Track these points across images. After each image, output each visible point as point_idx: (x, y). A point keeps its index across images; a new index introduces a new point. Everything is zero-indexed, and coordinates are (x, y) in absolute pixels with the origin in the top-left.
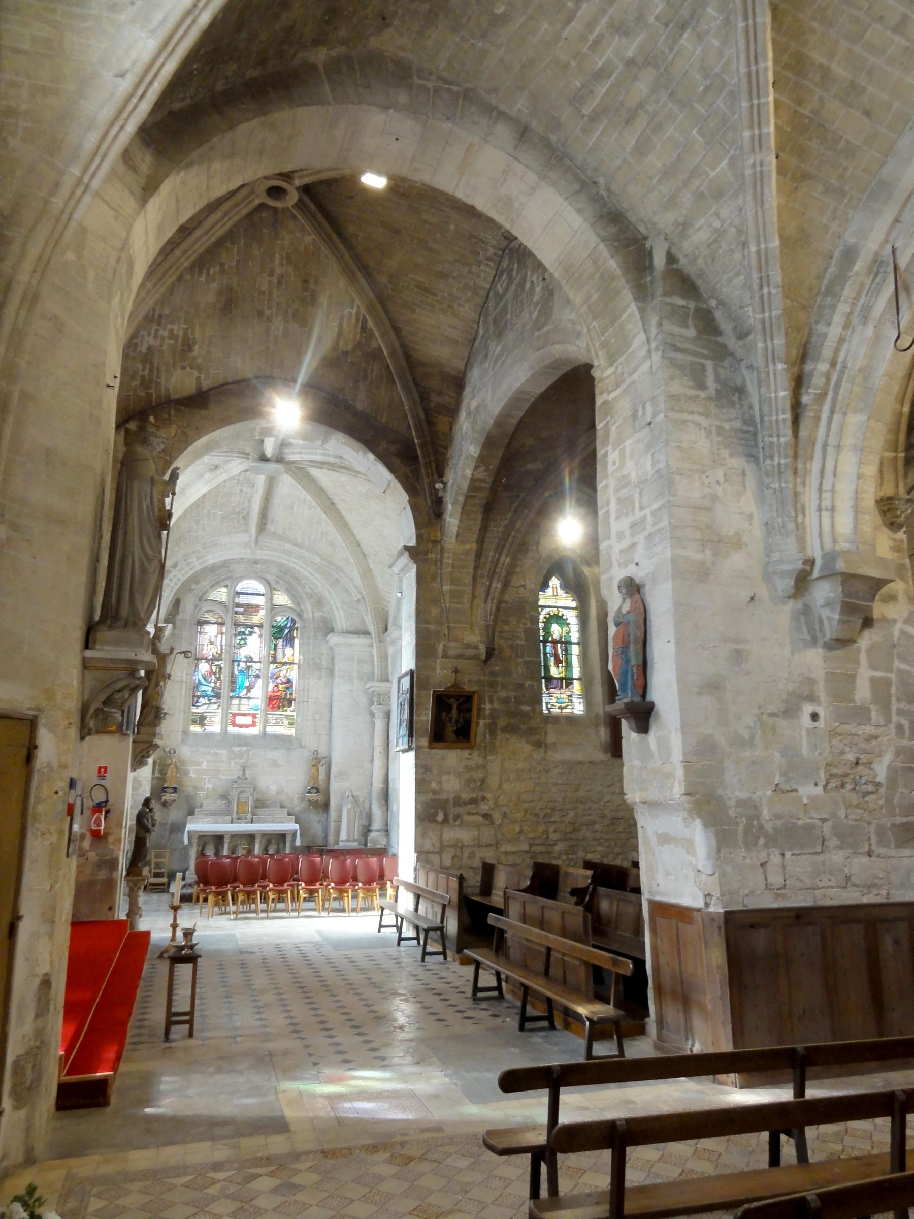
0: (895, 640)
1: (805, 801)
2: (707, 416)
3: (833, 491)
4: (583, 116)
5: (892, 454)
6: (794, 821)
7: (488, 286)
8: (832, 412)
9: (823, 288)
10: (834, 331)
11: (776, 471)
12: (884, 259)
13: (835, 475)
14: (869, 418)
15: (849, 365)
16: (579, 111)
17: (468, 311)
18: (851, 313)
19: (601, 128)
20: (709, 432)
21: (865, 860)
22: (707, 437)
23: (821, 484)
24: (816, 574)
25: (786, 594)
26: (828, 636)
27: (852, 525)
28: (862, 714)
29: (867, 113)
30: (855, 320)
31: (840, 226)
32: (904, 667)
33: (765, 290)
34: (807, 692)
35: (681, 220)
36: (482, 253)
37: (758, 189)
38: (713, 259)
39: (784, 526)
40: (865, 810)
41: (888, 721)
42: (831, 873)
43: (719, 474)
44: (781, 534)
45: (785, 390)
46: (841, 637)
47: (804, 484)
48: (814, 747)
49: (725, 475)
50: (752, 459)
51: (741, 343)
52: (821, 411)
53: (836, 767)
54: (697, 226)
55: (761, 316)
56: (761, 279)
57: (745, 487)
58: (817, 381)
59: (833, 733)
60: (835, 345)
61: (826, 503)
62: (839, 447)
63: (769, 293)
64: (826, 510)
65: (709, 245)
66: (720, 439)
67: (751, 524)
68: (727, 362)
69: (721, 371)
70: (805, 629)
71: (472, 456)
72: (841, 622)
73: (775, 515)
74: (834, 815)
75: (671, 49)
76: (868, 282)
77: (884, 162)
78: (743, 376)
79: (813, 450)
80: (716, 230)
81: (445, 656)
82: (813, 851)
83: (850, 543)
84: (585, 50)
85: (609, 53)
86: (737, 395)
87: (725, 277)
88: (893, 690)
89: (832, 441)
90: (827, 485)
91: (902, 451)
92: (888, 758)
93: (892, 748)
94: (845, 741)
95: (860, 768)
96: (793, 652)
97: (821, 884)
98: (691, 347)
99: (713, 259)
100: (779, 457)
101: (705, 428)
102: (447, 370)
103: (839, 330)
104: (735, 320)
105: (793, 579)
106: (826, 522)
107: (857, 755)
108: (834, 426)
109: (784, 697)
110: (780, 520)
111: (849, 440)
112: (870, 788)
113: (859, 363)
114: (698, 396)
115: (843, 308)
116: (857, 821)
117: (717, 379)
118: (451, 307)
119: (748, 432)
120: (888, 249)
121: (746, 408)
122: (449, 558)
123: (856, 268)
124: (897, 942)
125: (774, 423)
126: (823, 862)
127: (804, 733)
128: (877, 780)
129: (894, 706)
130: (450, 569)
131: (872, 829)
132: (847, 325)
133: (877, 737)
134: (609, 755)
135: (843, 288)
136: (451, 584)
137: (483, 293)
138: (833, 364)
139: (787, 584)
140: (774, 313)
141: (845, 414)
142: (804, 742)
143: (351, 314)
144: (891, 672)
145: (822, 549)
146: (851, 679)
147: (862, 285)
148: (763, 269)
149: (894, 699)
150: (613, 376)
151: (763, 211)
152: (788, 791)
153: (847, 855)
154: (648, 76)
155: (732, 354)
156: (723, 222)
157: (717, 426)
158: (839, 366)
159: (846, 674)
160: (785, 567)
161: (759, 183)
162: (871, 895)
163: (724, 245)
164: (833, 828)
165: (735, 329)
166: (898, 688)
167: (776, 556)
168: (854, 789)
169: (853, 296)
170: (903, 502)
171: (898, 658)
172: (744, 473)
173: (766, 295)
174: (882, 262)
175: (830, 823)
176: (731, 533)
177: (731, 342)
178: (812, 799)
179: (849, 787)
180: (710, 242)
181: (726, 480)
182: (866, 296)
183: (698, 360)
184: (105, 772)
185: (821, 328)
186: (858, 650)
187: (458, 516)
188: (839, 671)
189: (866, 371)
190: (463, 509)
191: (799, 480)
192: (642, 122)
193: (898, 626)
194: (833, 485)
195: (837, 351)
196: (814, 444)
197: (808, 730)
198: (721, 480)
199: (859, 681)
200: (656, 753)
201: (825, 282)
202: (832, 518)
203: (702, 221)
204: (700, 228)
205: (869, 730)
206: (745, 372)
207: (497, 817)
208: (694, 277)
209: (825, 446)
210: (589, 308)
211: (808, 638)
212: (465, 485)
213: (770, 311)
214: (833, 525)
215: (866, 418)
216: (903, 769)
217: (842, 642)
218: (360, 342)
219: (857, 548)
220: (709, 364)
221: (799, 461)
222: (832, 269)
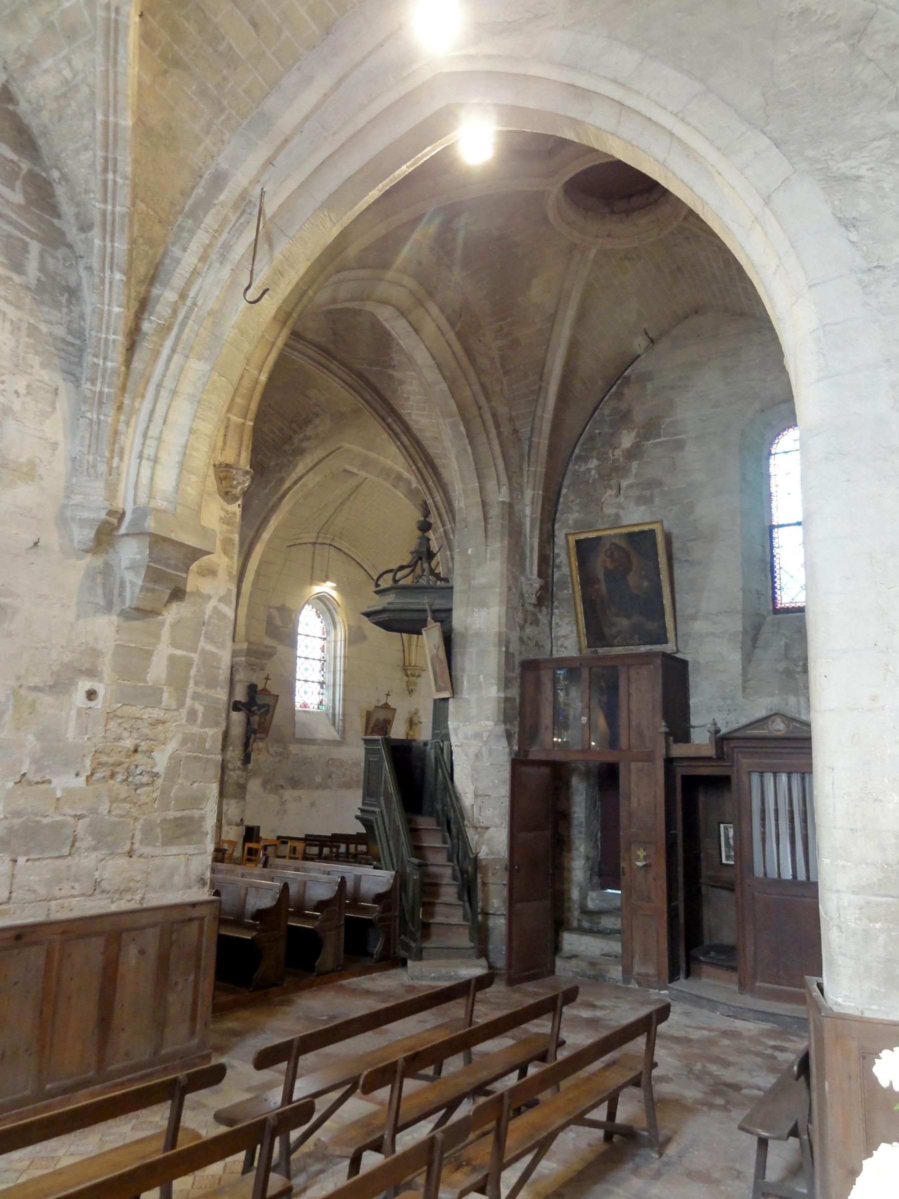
0: (206, 617)
1: (59, 794)
2: (18, 308)
3: (159, 439)
5: (241, 420)
6: (38, 818)
8: (173, 351)
9: (187, 208)
10: (189, 259)
11: (96, 399)
12: (252, 198)
13: (164, 423)
14: (212, 370)
15: (199, 303)
18: (210, 246)
20: (15, 329)
21: (123, 861)
22: (12, 333)
23: (148, 427)
24: (123, 530)
25: (83, 547)
26: (128, 603)
27: (174, 483)
28: (152, 696)
29: (255, 25)
30: (214, 255)
31: (214, 144)
32: (210, 648)
33: (110, 176)
34: (87, 666)
37: (112, 43)
38: (60, 118)
39: (94, 466)
40: (135, 803)
41: (181, 704)
42: (76, 880)
43: (21, 384)
44: (89, 475)
45: (120, 306)
46: (141, 607)
47: (128, 424)
48: (83, 730)
49: (28, 386)
50: (71, 378)
51: (83, 236)
52: (161, 346)
53: (108, 755)
55: (102, 206)
56: (106, 159)
57: (53, 405)
58: (161, 310)
59: (111, 715)
60: (187, 275)
61: (149, 451)
62: (174, 392)
63: (115, 182)
64: (148, 459)
65: (57, 98)
66: (32, 341)
67: (53, 455)
68: (61, 252)
69: (50, 261)
70: (100, 591)
72: (143, 588)
73: (85, 450)
74: (94, 810)
76: (234, 219)
77: (268, 94)
78: (80, 277)
79: (145, 388)
80: (66, 82)
82: (57, 854)
83: (170, 502)
86: (66, 295)
87: (71, 146)
88: (193, 672)
89: (168, 383)
90: (154, 432)
91: (251, 420)
92: (172, 746)
93: (180, 735)
94: (125, 725)
95: (138, 756)
96: (78, 617)
97: (57, 893)
98: (14, 216)
99: (60, 118)
100: (102, 383)
101: (12, 322)
103: (195, 260)
104: (78, 205)
105: (95, 531)
106: (146, 472)
107: (138, 741)
108: (172, 366)
109: (55, 668)
110: (91, 458)
111: (187, 388)
112: (145, 779)
113: (211, 305)
114: (11, 279)
115: (201, 238)
116: (122, 816)
117: (42, 268)
119: (73, 345)
120: (258, 191)
121: (75, 315)
123: (222, 197)
124: (142, 952)
125: (102, 342)
126: (69, 867)
127: (73, 713)
128: (155, 770)
129: (191, 689)
131: (139, 825)
132: (203, 258)
133: (164, 723)
135: (205, 214)
138: (183, 296)
139: (84, 535)
140: (118, 209)
141: (187, 357)
142: (72, 724)
144: (195, 652)
145: (135, 502)
146: (147, 654)
147: (226, 218)
148: (111, 147)
149: (192, 681)
151: (116, 73)
152: (38, 783)
153: (101, 857)
155: (70, 246)
156: (75, 74)
157: (29, 324)
158: (189, 302)
159: (141, 649)
160: (86, 514)
161: (112, 34)
162: (123, 902)
163: (73, 104)
164: (90, 825)
165: (77, 215)
166: (198, 671)
167: (77, 499)
168: (126, 780)
169: (216, 227)
170: (240, 473)
171: (206, 638)
172: (56, 392)
173: (110, 183)
174: (250, 201)
175: (86, 821)
176: (23, 459)
177: (72, 234)
178: (68, 791)
179: (120, 777)
180: (59, 93)
181: (28, 393)
182: (229, 233)
183: (18, 234)
185: (176, 250)
186: (162, 624)
188: (133, 645)
189: (217, 316)
191: (122, 418)
193: (213, 603)
194: (161, 433)
195: (189, 283)
196: (148, 382)
197: (79, 710)
198: (23, 391)
199: (155, 658)
201: (190, 202)
202: (153, 469)
203: (48, 63)
204: (46, 71)
205: (157, 713)
206: (83, 274)
208: (35, 130)
209: (159, 386)
211: (101, 601)
213: (114, 205)
214: (152, 478)
215: (208, 368)
216: (187, 757)
217: (142, 613)
219: (175, 509)
220: (35, 247)
221: (126, 395)
222: (199, 191)
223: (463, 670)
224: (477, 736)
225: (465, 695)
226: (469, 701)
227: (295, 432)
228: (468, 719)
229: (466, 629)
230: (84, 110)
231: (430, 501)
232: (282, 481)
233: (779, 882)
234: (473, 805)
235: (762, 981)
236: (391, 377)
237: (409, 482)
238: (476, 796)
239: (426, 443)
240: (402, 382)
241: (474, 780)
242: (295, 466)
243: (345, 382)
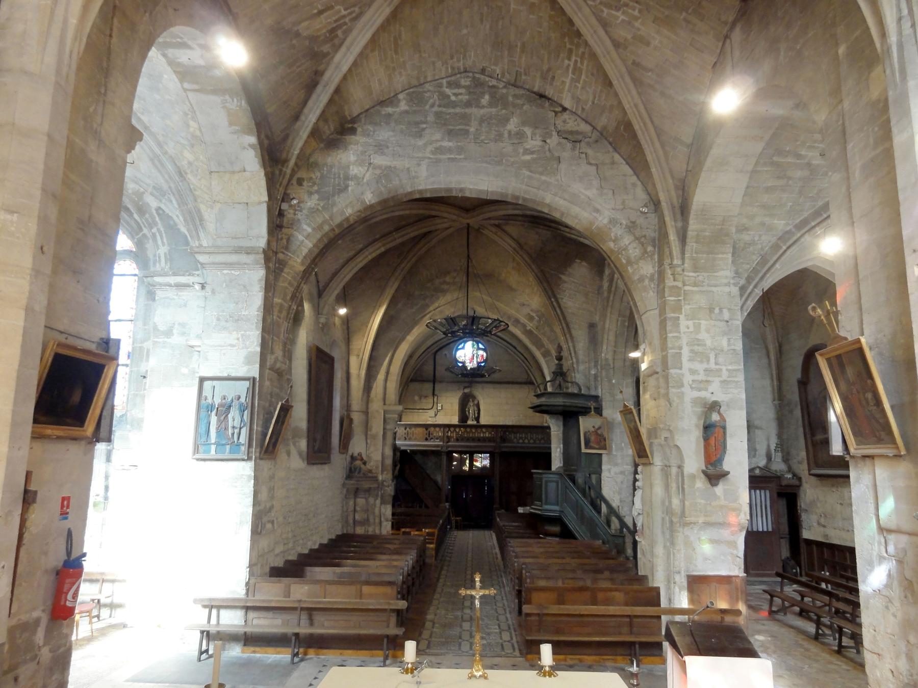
4: (772, 159)
7: (429, 79)
16: (773, 156)
17: (400, 80)
19: (769, 169)
35: (746, 226)
36: (455, 60)
38: (743, 250)
54: (749, 233)
65: (745, 243)
71: (363, 202)
75: (822, 175)
81: (271, 369)
84: (808, 144)
85: (810, 154)
87: (742, 261)
102: (346, 108)
118: (394, 69)
122: (288, 273)
130: (286, 285)
134: (306, 462)
136: (282, 299)
137: (422, 81)
143: (339, 11)
150: (693, 278)
154: (806, 173)
163: (751, 248)
184: (68, 507)
187: (315, 241)
190: (322, 237)
192: (781, 182)
200: (722, 497)
207: (275, 522)
210: (698, 235)
212: (338, 220)
218: (318, 37)
223: (612, 440)
224: (622, 473)
225: (614, 453)
226: (616, 456)
227: (437, 277)
228: (616, 465)
229: (613, 419)
230: (756, 252)
231: (564, 347)
232: (427, 306)
233: (758, 532)
234: (619, 507)
235: (753, 570)
236: (560, 278)
237: (524, 326)
238: (621, 501)
239: (566, 314)
240: (565, 282)
241: (619, 493)
242: (438, 299)
243: (536, 275)
